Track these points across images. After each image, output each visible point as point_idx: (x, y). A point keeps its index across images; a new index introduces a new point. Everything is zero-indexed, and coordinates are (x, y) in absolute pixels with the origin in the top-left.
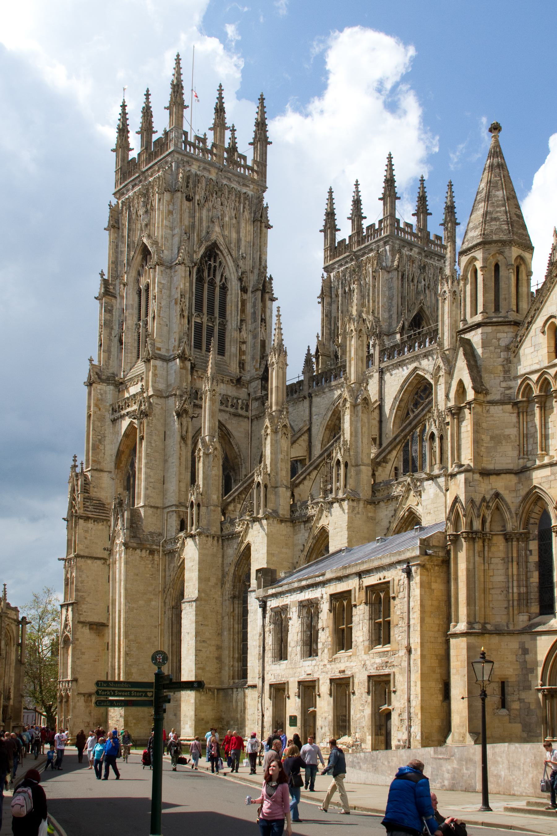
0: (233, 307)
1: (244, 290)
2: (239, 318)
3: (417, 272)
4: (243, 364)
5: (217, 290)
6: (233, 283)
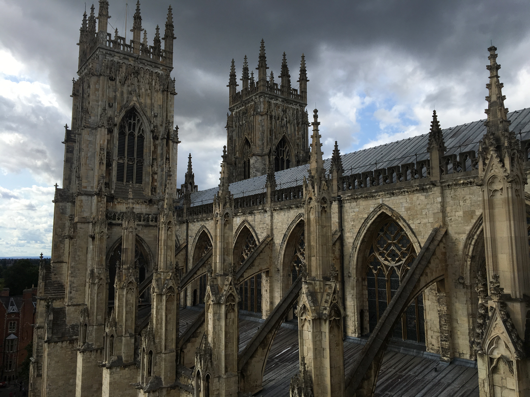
0: (147, 150)
1: (155, 138)
2: (151, 158)
3: (281, 114)
4: (155, 189)
5: (136, 139)
6: (148, 134)
